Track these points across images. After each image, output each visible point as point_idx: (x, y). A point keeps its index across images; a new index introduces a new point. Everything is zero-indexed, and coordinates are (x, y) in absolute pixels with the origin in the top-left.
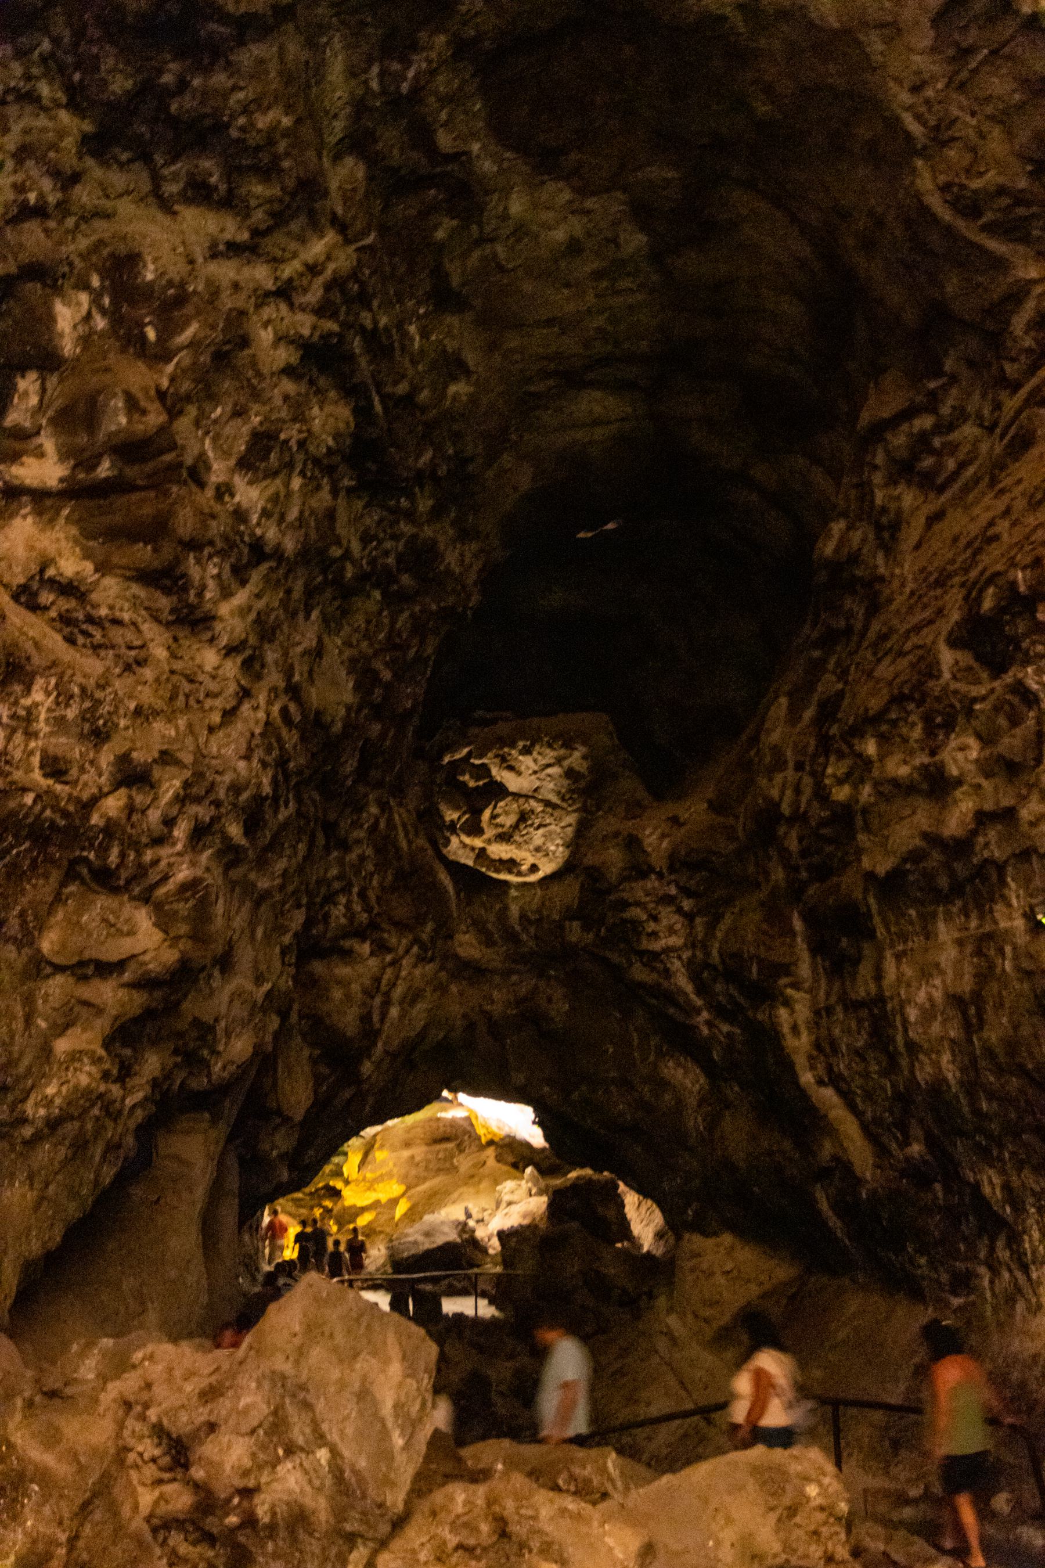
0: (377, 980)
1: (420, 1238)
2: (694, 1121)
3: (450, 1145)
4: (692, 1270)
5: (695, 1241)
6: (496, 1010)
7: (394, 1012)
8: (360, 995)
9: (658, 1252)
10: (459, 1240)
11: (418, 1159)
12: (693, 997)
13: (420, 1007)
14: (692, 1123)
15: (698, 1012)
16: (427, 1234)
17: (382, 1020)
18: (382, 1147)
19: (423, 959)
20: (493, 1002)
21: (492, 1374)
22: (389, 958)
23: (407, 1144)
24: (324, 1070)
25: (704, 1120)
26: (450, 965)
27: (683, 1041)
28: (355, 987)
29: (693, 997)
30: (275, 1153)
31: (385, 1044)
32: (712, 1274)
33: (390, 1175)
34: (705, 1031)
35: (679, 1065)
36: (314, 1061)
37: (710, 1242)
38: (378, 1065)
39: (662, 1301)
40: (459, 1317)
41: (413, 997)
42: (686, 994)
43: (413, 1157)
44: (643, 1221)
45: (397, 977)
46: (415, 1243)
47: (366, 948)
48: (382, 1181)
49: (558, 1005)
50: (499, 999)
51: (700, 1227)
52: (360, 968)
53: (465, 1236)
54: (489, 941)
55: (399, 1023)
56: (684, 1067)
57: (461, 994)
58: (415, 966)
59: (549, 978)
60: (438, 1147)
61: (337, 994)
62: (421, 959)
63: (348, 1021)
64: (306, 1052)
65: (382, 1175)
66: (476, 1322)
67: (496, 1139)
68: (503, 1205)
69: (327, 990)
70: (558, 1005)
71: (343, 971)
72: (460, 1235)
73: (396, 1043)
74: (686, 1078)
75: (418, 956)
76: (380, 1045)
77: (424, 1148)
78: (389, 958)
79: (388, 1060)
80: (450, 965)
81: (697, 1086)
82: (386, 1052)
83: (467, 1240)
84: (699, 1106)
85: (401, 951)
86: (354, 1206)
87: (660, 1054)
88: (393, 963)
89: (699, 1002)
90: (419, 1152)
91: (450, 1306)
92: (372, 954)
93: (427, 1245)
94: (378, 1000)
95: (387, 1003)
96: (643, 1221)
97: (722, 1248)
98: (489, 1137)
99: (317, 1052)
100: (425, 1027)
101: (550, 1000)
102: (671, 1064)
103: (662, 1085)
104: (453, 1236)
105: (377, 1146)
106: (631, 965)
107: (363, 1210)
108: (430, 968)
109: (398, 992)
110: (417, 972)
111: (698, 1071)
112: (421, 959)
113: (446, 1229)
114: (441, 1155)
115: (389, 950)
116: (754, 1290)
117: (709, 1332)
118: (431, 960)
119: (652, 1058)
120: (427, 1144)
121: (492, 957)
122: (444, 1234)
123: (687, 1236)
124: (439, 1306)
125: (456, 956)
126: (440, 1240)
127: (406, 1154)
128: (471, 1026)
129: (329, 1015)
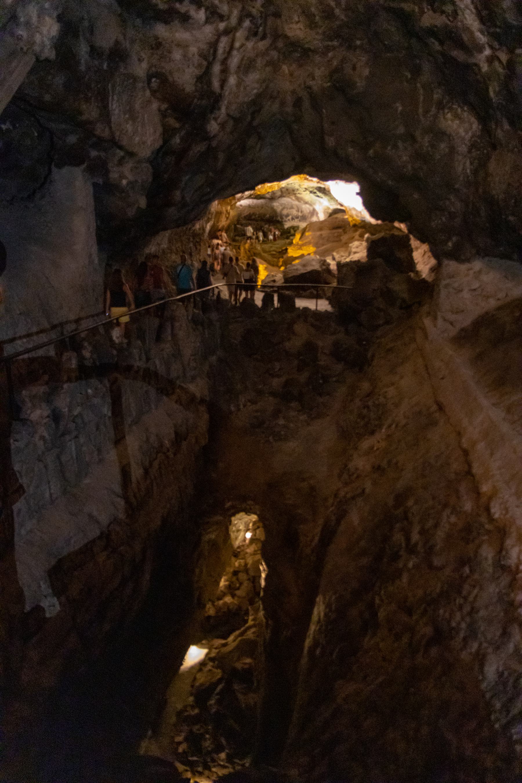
0: (214, 45)
1: (299, 267)
2: (463, 166)
3: (340, 230)
4: (447, 286)
5: (451, 266)
6: (316, 85)
7: (232, 80)
8: (197, 57)
9: (430, 280)
10: (320, 269)
11: (324, 236)
12: (478, 34)
13: (253, 77)
14: (460, 169)
15: (480, 49)
16: (304, 266)
17: (222, 87)
18: (309, 231)
19: (256, 34)
20: (314, 79)
21: (320, 344)
22: (222, 26)
23: (321, 229)
24: (172, 122)
25: (471, 163)
26: (280, 44)
27: (462, 84)
28: (193, 50)
29: (478, 34)
30: (124, 182)
31: (227, 108)
32: (461, 291)
33: (309, 243)
34: (485, 68)
35: (456, 116)
36: (163, 115)
37: (463, 267)
38: (223, 126)
39: (425, 308)
40: (306, 309)
41: (247, 66)
42: (472, 33)
43: (321, 235)
44: (422, 258)
45: (232, 48)
46: (297, 270)
47: (201, 15)
48: (305, 245)
49: (361, 70)
50: (317, 75)
51: (456, 255)
52: (197, 34)
53: (324, 267)
54: (312, 25)
55: (237, 88)
56: (460, 119)
57: (291, 75)
58: (247, 39)
59: (356, 48)
60: (335, 231)
61: (177, 55)
62: (253, 33)
63: (186, 78)
64: (155, 105)
65: (306, 243)
66: (317, 315)
67: (357, 224)
68: (352, 253)
69: (170, 52)
70: (361, 70)
71: (182, 35)
72: (321, 267)
73: (233, 107)
74: (460, 126)
75: (250, 29)
76: (223, 110)
77: (329, 231)
78: (222, 26)
79: (231, 123)
80: (280, 44)
81: (470, 134)
82: (228, 115)
83: (324, 270)
84: (470, 151)
85: (234, 21)
86: (292, 256)
87: (441, 106)
88: (227, 32)
89: (482, 39)
90: (325, 233)
91: (300, 303)
92: (207, 21)
93: (303, 271)
94: (217, 68)
95: (225, 71)
96: (422, 258)
97: (471, 272)
98: (354, 222)
99: (164, 106)
100: (259, 96)
101: (354, 68)
102: (449, 116)
103: (440, 135)
104: (316, 267)
105: (307, 230)
106: (422, 12)
107: (296, 258)
108: (262, 45)
109: (234, 61)
110: (250, 45)
111: (473, 119)
112: (253, 33)
113: (314, 263)
114: (336, 235)
115: (222, 18)
116: (493, 303)
117: (453, 332)
118: (263, 38)
119: (434, 110)
120: (330, 230)
121: (313, 39)
122: (313, 266)
123: (446, 262)
124: (294, 302)
125: (286, 37)
126: (309, 269)
127: (318, 233)
128: (298, 102)
129: (171, 73)
